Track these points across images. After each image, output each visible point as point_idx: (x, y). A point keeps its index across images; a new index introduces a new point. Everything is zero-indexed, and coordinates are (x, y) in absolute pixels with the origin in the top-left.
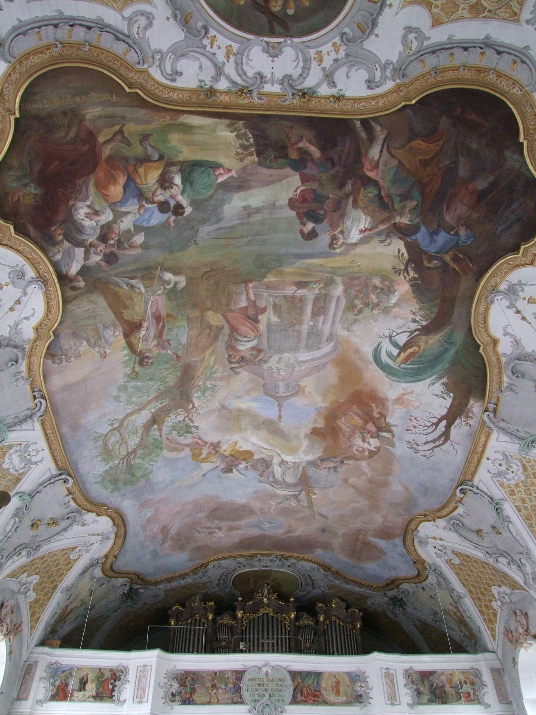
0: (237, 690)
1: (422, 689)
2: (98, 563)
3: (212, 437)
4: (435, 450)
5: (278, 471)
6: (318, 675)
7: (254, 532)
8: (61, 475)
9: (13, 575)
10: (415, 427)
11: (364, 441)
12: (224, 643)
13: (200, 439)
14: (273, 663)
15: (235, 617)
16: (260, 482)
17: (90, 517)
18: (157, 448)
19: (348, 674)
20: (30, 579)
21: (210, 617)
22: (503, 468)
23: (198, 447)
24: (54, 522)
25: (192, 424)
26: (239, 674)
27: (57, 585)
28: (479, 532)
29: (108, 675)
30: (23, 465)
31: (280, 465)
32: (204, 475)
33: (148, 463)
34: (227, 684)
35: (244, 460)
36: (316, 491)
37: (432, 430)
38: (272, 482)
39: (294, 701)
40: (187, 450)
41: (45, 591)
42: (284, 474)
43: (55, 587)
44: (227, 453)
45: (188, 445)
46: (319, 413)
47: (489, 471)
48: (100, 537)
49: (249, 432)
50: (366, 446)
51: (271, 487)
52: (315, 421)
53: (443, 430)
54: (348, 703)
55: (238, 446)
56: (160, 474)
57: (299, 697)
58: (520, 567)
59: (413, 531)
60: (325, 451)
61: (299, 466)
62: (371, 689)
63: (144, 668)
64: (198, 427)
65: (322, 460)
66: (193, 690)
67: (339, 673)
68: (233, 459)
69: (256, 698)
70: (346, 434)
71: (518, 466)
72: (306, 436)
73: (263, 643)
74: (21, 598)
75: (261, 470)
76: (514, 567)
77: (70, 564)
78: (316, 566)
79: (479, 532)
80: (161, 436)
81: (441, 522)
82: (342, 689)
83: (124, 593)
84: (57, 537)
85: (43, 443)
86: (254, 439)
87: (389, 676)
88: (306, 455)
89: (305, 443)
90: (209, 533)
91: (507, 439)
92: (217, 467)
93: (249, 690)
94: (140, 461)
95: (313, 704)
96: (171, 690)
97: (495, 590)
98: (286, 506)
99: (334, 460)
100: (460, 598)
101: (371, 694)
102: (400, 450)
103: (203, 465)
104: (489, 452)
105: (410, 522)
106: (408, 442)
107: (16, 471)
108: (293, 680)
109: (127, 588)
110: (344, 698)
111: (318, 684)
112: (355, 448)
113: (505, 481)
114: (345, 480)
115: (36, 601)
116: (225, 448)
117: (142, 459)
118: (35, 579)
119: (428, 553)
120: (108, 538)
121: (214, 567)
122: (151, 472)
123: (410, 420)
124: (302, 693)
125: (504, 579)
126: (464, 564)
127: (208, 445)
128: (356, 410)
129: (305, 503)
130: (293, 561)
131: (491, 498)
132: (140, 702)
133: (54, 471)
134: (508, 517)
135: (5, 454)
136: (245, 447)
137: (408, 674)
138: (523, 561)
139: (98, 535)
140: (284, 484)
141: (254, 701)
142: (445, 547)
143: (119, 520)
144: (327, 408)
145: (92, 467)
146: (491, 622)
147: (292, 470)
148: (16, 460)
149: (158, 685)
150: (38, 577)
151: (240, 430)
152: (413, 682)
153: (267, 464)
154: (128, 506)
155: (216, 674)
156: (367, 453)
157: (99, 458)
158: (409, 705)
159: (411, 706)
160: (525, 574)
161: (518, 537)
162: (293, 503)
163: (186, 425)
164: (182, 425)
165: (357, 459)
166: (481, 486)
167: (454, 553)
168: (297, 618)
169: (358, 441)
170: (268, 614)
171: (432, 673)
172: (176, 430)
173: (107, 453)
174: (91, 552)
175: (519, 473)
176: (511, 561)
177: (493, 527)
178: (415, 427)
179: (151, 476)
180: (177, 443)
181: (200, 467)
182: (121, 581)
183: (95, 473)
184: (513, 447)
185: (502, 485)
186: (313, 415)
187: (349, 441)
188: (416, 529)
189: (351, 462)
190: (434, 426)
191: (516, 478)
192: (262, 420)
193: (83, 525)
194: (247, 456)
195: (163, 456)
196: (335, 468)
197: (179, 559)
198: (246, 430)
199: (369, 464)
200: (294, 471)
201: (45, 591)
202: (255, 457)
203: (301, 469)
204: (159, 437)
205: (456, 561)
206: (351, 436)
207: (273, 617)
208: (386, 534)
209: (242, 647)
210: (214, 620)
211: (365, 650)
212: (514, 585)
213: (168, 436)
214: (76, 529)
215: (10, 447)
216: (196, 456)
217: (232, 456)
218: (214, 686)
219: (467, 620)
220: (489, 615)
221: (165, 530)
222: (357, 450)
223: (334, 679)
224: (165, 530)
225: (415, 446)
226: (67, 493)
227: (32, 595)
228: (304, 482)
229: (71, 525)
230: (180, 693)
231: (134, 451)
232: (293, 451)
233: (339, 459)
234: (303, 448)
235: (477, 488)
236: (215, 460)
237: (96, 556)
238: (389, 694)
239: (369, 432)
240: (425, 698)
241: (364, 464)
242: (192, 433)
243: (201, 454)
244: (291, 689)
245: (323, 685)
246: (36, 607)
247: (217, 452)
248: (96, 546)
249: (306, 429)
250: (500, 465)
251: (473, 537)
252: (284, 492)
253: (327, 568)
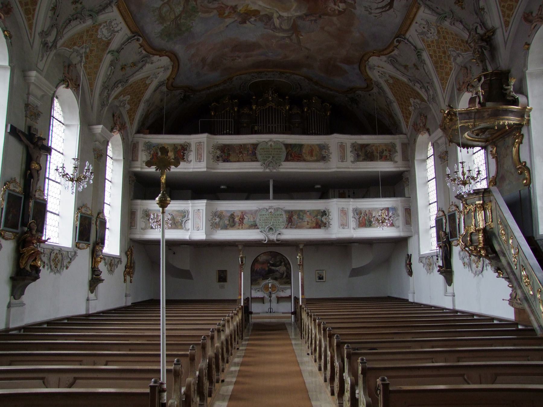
0: (254, 154)
1: (360, 153)
2: (163, 84)
4: (383, 13)
5: (277, 22)
6: (301, 146)
7: (262, 58)
8: (134, 36)
9: (116, 98)
11: (335, 4)
12: (245, 125)
14: (275, 140)
15: (251, 109)
16: (265, 28)
17: (156, 58)
19: (319, 145)
20: (125, 98)
21: (236, 110)
22: (425, 30)
24: (134, 64)
26: (255, 146)
27: (141, 99)
28: (406, 67)
29: (179, 147)
30: (110, 34)
31: (278, 18)
32: (227, 26)
34: (248, 151)
39: (287, 160)
40: (215, 12)
41: (135, 104)
42: (281, 24)
43: (140, 101)
44: (242, 12)
45: (214, 9)
47: (416, 30)
48: (163, 69)
50: (336, 7)
54: (317, 161)
56: (198, 27)
57: (290, 158)
58: (427, 91)
59: (366, 61)
62: (331, 153)
63: (199, 144)
66: (229, 155)
67: (313, 145)
69: (265, 158)
71: (434, 30)
73: (269, 127)
74: (121, 109)
76: (423, 90)
77: (146, 86)
78: (302, 78)
79: (406, 67)
80: (196, 4)
81: (384, 58)
82: (314, 154)
83: (181, 99)
84: (137, 73)
85: (120, 19)
87: (342, 147)
90: (232, 60)
91: (429, 12)
93: (261, 154)
94: (184, 21)
95: (297, 161)
96: (217, 155)
97: (412, 100)
100: (391, 102)
101: (331, 156)
102: (359, 11)
103: (226, 20)
104: (418, 19)
105: (363, 57)
107: (106, 38)
108: (286, 149)
109: (183, 95)
110: (315, 158)
111: (301, 151)
112: (329, 8)
113: (425, 38)
115: (131, 109)
116: (241, 9)
118: (128, 98)
119: (374, 75)
120: (168, 69)
121: (236, 79)
124: (291, 155)
125: (417, 95)
126: (395, 84)
130: (288, 74)
131: (415, 47)
132: (200, 161)
133: (130, 34)
134: (424, 60)
135: (98, 30)
137: (353, 146)
138: (429, 87)
139: (162, 67)
140: (281, 30)
141: (264, 160)
142: (385, 73)
143: (174, 57)
145: (153, 29)
146: (407, 118)
148: (105, 31)
149: (209, 152)
150: (129, 96)
152: (355, 150)
153: (269, 18)
154: (178, 48)
155: (241, 145)
156: (337, 12)
157: (157, 22)
158: (352, 162)
159: (352, 162)
160: (429, 95)
161: (428, 73)
162: (287, 41)
166: (411, 40)
167: (390, 76)
168: (290, 109)
169: (332, 5)
170: (272, 107)
171: (367, 145)
173: (162, 19)
174: (158, 78)
175: (435, 34)
176: (423, 87)
177: (415, 65)
182: (179, 91)
183: (156, 31)
184: (433, 18)
185: (423, 40)
188: (367, 60)
189: (326, 17)
191: (433, 37)
193: (152, 63)
194: (256, 13)
196: (315, 20)
197: (214, 76)
201: (135, 104)
202: (261, 14)
203: (292, 21)
205: (391, 81)
207: (275, 109)
208: (348, 61)
209: (256, 128)
210: (238, 111)
211: (330, 131)
212: (422, 100)
214: (148, 66)
215: (100, 25)
216: (221, 14)
217: (246, 13)
218: (241, 152)
219: (394, 115)
220: (406, 114)
221: (204, 60)
222: (330, 10)
223: (310, 148)
224: (204, 60)
225: (370, 10)
226: (139, 46)
227: (128, 107)
228: (295, 28)
229: (144, 65)
230: (222, 156)
231: (180, 15)
233: (318, 15)
234: (294, 8)
235: (408, 40)
237: (162, 80)
238: (341, 156)
240: (361, 158)
241: (335, 19)
243: (225, 13)
244: (285, 154)
245: (304, 151)
246: (131, 113)
247: (235, 12)
248: (161, 74)
250: (424, 28)
251: (402, 69)
252: (281, 35)
253: (310, 79)
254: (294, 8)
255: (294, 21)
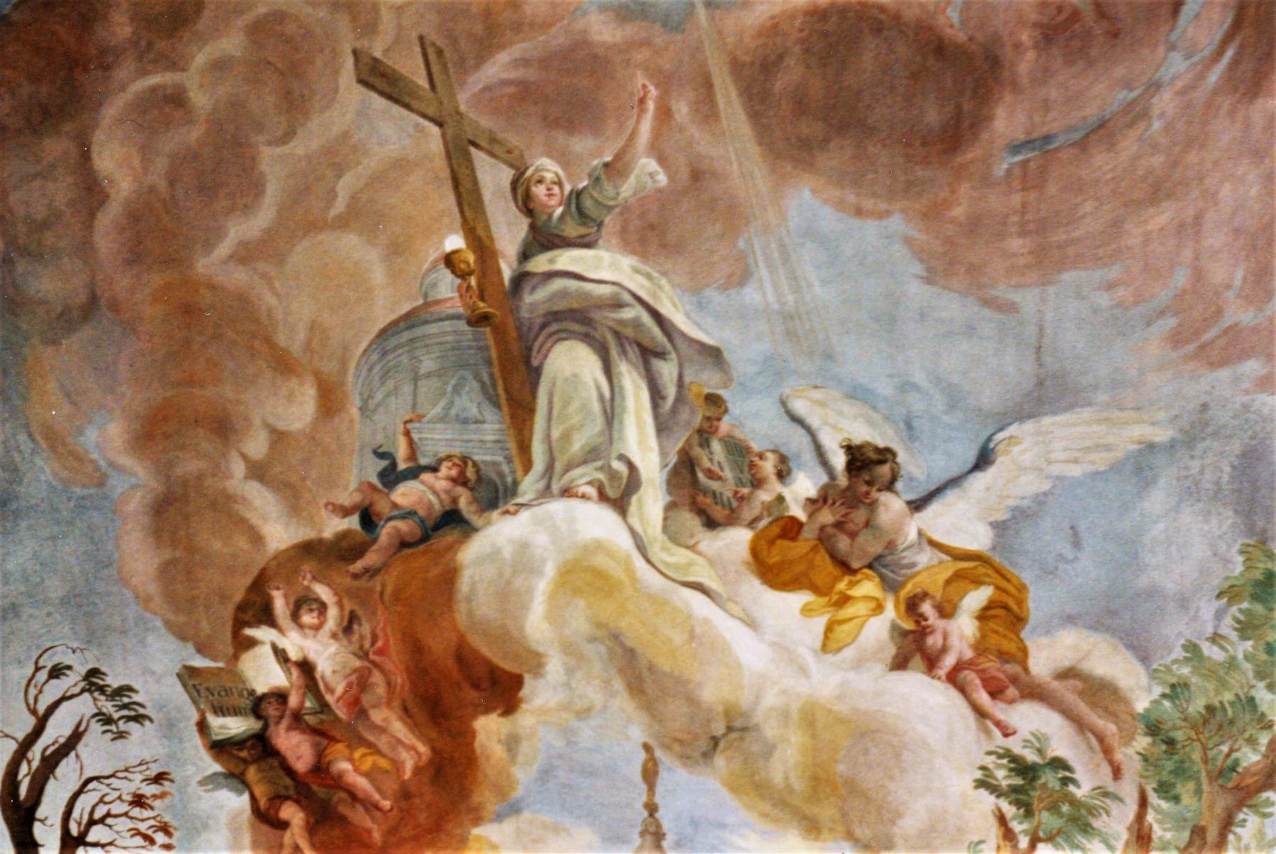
3: (924, 702)
10: (139, 801)
11: (306, 667)
13: (980, 713)
16: (714, 355)
18: (1171, 742)
23: (991, 665)
25: (1009, 810)
32: (983, 460)
33: (1232, 664)
35: (791, 529)
36: (446, 286)
37: (76, 814)
38: (661, 355)
44: (868, 587)
45: (1034, 692)
46: (502, 791)
49: (771, 699)
50: (294, 643)
51: (666, 309)
52: (512, 743)
53: (38, 831)
55: (820, 623)
60: (450, 577)
61: (550, 468)
64: (981, 784)
65: (451, 519)
68: (843, 543)
70: (381, 690)
72: (536, 663)
75: (716, 446)
86: (750, 651)
88: (523, 547)
89: (536, 625)
92: (917, 505)
98: (581, 144)
99: (402, 526)
102: (154, 665)
103: (977, 538)
106: (138, 719)
112: (333, 612)
114: (330, 401)
117: (1251, 700)
122: (1230, 593)
123: (165, 829)
127: (949, 661)
128: (368, 823)
129: (493, 177)
136: (786, 608)
144: (477, 821)
147: (578, 444)
151: (810, 717)
156: (280, 605)
163: (1029, 813)
164: (1047, 820)
165: (308, 549)
172: (1074, 802)
178: (139, 801)
179: (1238, 566)
180: (1080, 725)
181: (1000, 528)
186: (523, 776)
187: (362, 654)
190: (74, 830)
192: (720, 761)
195: (1154, 675)
196: (391, 477)
198: (785, 715)
199: (257, 539)
200: (566, 437)
202: (738, 539)
204: (1153, 799)
206: (361, 683)
213: (1111, 786)
216: (1006, 615)
217: (845, 567)
222: (323, 608)
225: (108, 707)
232: (584, 575)
233: (386, 532)
236: (925, 558)
239: (297, 719)
241: (280, 534)
242: (1014, 759)
243: (984, 615)
247: (912, 607)
249: (541, 695)
252: (605, 267)
254: (542, 586)
255: (528, 466)
